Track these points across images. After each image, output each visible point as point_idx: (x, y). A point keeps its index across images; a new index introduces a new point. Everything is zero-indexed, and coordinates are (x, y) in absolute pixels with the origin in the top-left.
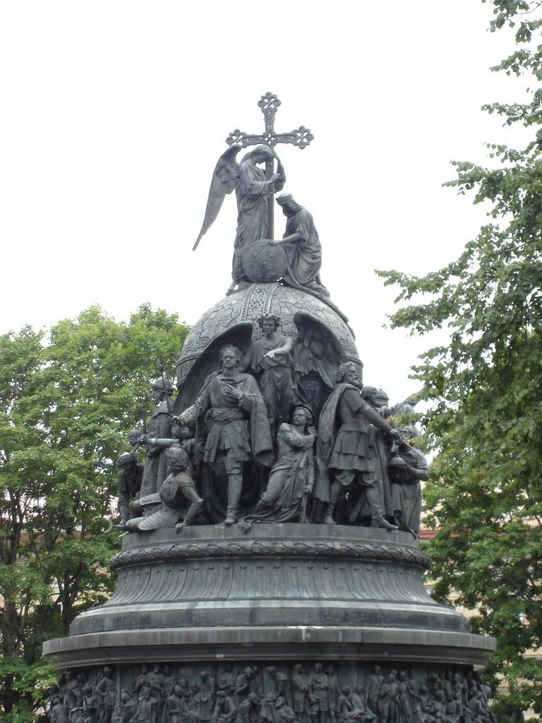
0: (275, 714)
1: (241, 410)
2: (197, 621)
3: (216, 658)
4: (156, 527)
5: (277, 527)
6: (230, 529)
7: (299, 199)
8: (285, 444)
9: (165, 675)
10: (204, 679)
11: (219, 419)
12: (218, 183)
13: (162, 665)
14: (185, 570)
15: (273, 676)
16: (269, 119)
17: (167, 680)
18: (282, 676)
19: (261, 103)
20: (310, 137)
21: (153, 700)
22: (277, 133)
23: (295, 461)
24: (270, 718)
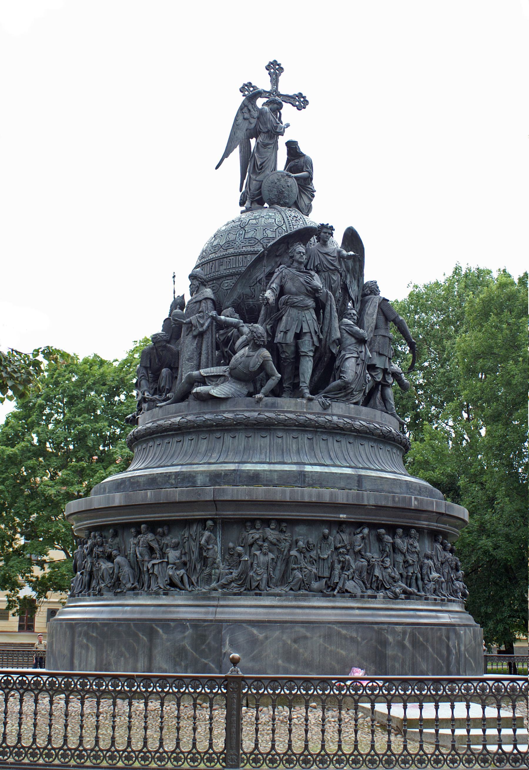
0: (384, 574)
1: (317, 300)
2: (311, 482)
3: (339, 518)
4: (231, 396)
5: (349, 407)
6: (311, 403)
7: (304, 148)
8: (349, 337)
9: (282, 531)
10: (325, 538)
11: (299, 305)
12: (241, 118)
13: (280, 521)
14: (269, 437)
15: (380, 539)
16: (275, 81)
17: (282, 537)
18: (388, 538)
19: (268, 68)
20: (306, 102)
21: (271, 556)
22: (281, 93)
23: (361, 352)
24: (381, 578)
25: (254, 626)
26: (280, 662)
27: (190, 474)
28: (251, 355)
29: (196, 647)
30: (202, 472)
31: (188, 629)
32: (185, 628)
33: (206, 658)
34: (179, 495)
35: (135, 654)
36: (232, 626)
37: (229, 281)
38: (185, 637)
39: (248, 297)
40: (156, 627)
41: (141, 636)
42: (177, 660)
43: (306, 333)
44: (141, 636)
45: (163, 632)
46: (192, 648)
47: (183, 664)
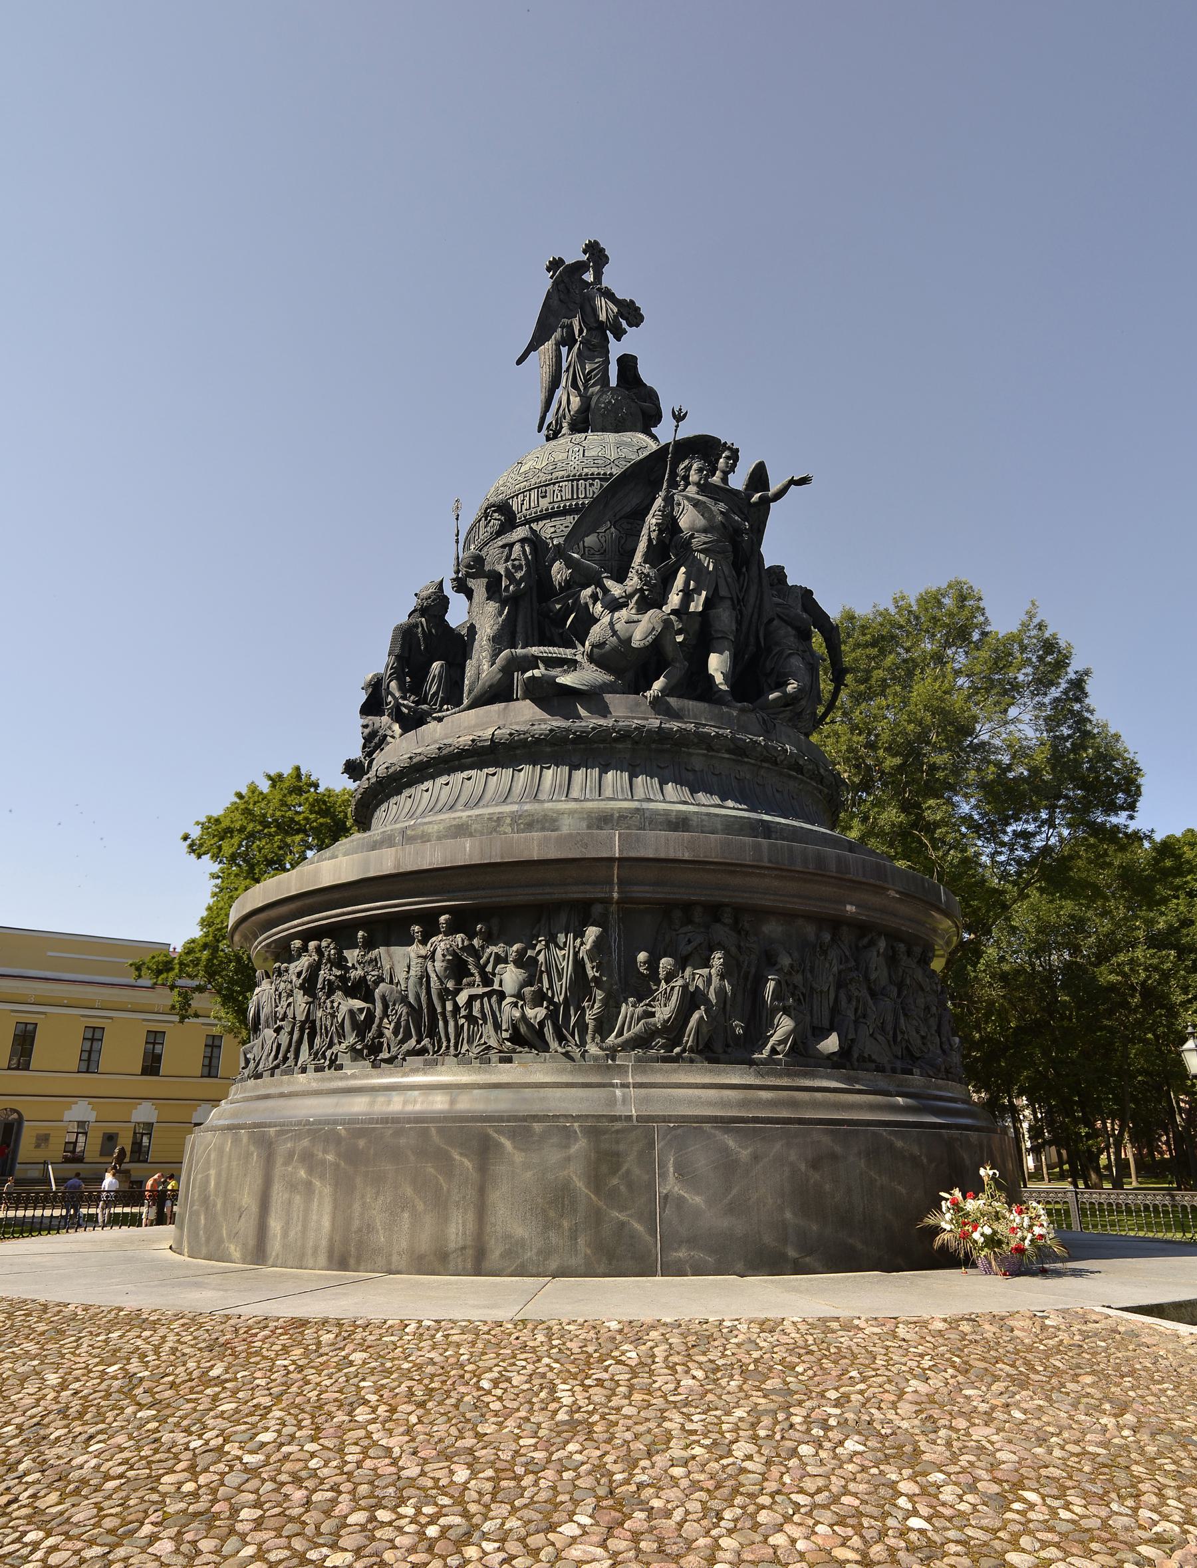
25: (727, 1131)
26: (788, 1215)
27: (546, 815)
28: (635, 619)
29: (596, 1181)
30: (572, 813)
31: (576, 1139)
32: (568, 1135)
33: (622, 1209)
34: (539, 846)
35: (440, 1204)
36: (679, 1131)
37: (559, 523)
38: (568, 1159)
39: (592, 551)
40: (495, 1135)
41: (457, 1157)
42: (552, 1214)
43: (723, 598)
44: (457, 1157)
45: (515, 1148)
46: (588, 1186)
47: (566, 1224)
